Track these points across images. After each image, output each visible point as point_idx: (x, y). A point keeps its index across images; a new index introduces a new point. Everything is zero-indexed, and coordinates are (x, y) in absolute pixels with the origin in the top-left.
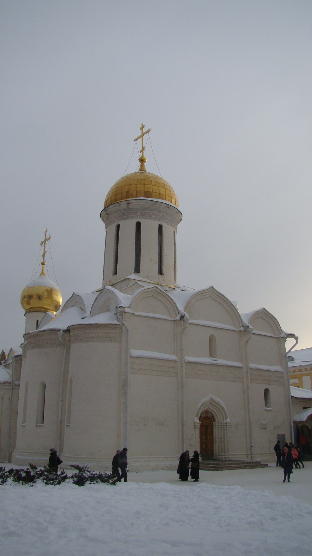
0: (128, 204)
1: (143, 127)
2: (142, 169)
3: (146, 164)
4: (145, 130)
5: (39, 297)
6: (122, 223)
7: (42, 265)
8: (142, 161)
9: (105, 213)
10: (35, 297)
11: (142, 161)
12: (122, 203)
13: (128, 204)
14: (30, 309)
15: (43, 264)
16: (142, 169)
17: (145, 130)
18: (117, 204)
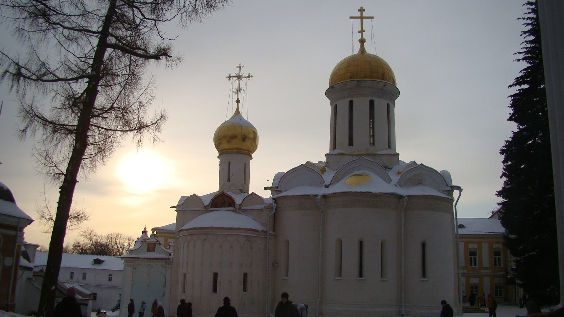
0: (385, 85)
1: (362, 10)
2: (362, 50)
3: (365, 44)
4: (364, 14)
5: (244, 138)
6: (377, 101)
7: (237, 103)
8: (362, 41)
9: (357, 84)
10: (239, 137)
11: (362, 41)
12: (381, 83)
13: (385, 85)
14: (238, 150)
15: (238, 101)
16: (362, 50)
17: (364, 14)
18: (376, 82)
